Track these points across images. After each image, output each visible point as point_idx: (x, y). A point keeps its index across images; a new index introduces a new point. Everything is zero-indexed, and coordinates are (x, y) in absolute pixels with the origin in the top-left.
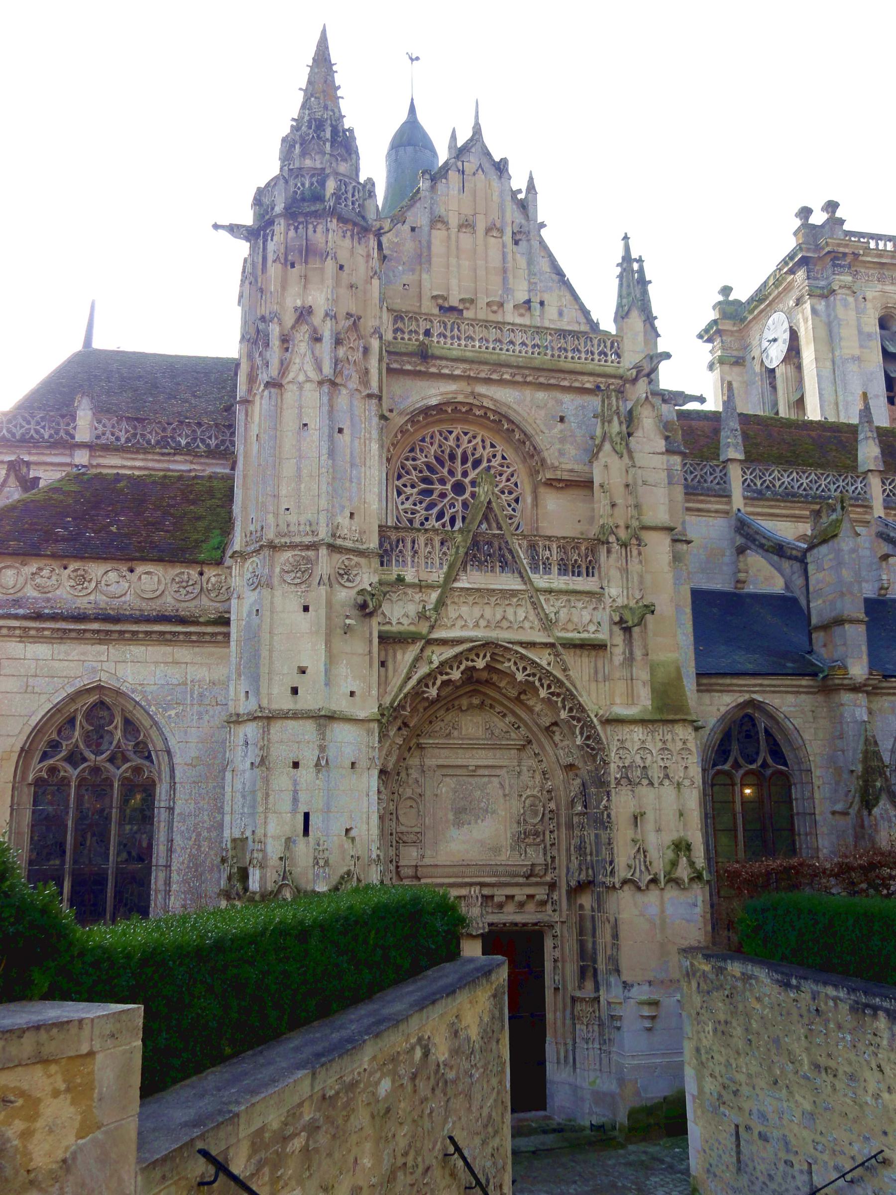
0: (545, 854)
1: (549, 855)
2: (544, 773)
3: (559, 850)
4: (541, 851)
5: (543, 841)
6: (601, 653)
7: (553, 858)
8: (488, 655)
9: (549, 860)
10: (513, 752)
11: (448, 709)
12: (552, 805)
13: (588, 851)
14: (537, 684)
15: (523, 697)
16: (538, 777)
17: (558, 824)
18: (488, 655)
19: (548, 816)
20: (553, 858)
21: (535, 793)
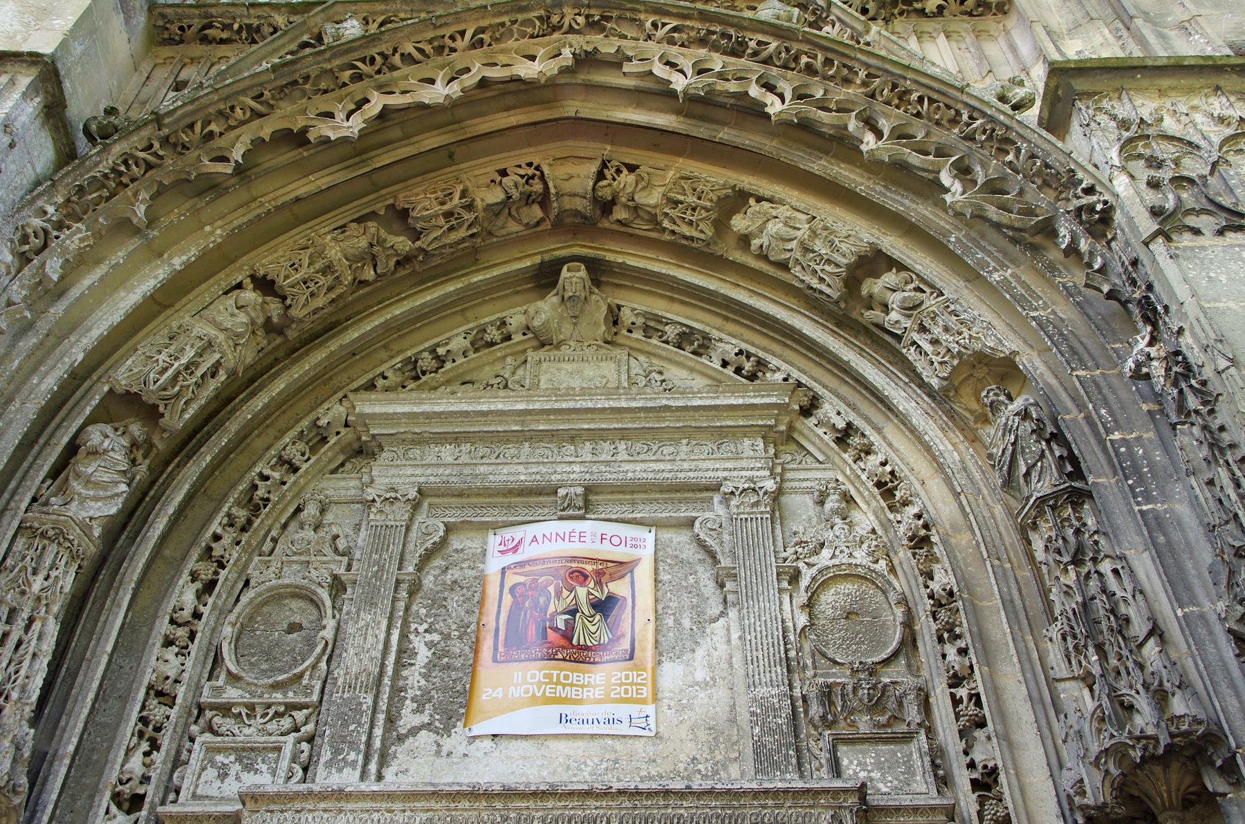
0: (944, 782)
1: (963, 778)
2: (886, 488)
3: (1006, 738)
4: (920, 764)
5: (930, 731)
6: (989, 22)
7: (986, 783)
8: (567, 52)
9: (968, 802)
10: (747, 442)
11: (480, 343)
12: (942, 579)
13: (1139, 628)
14: (755, 91)
15: (739, 223)
16: (865, 518)
17: (981, 636)
18: (567, 52)
19: (926, 628)
20: (986, 783)
21: (861, 557)
